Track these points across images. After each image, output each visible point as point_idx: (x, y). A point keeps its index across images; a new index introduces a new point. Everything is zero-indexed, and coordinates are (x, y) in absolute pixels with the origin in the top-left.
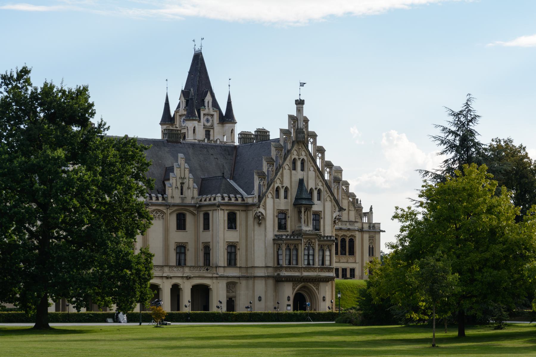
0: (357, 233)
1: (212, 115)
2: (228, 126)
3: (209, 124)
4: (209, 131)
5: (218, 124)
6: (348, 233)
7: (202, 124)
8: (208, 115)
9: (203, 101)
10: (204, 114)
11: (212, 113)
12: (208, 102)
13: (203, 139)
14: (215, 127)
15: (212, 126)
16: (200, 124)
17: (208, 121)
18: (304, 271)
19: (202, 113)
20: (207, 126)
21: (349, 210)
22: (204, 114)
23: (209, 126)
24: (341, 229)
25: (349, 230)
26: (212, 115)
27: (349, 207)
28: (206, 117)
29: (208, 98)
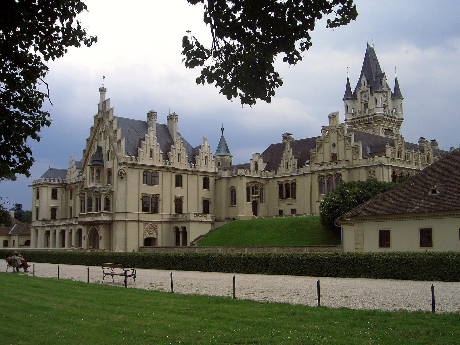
0: (344, 170)
1: (368, 91)
3: (367, 98)
4: (367, 104)
6: (334, 172)
7: (359, 100)
8: (365, 92)
10: (361, 92)
11: (366, 89)
16: (358, 100)
17: (365, 96)
18: (86, 217)
21: (345, 150)
22: (361, 92)
24: (325, 170)
25: (333, 169)
26: (368, 91)
27: (345, 147)
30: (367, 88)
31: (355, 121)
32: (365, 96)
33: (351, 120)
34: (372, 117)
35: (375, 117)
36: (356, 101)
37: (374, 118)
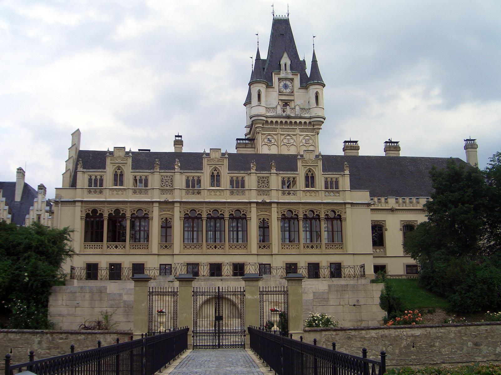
1: (292, 80)
2: (313, 89)
3: (288, 90)
5: (299, 88)
8: (286, 79)
9: (280, 65)
10: (279, 79)
11: (290, 76)
12: (285, 65)
13: (274, 106)
14: (295, 93)
15: (292, 93)
17: (286, 86)
19: (275, 78)
20: (284, 93)
23: (288, 93)
26: (292, 80)
28: (282, 84)
29: (285, 60)
30: (292, 75)
31: (274, 120)
32: (286, 86)
33: (267, 117)
34: (308, 121)
35: (313, 122)
36: (271, 90)
37: (310, 123)
